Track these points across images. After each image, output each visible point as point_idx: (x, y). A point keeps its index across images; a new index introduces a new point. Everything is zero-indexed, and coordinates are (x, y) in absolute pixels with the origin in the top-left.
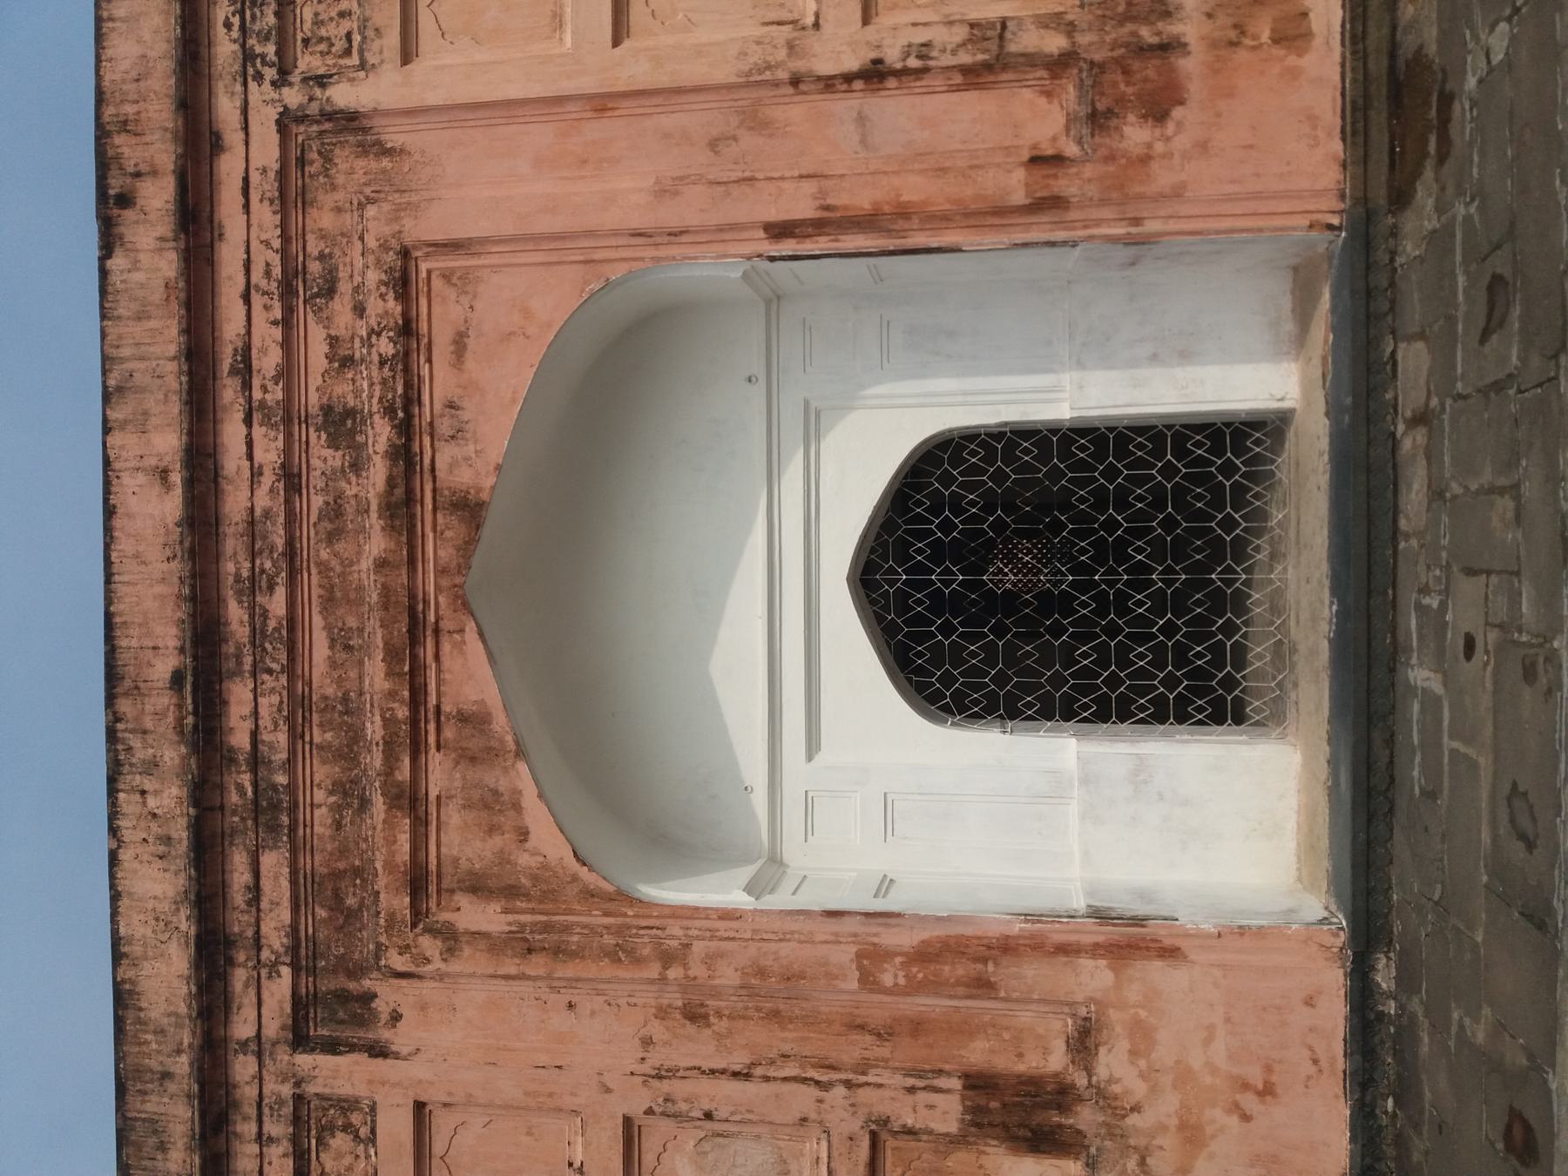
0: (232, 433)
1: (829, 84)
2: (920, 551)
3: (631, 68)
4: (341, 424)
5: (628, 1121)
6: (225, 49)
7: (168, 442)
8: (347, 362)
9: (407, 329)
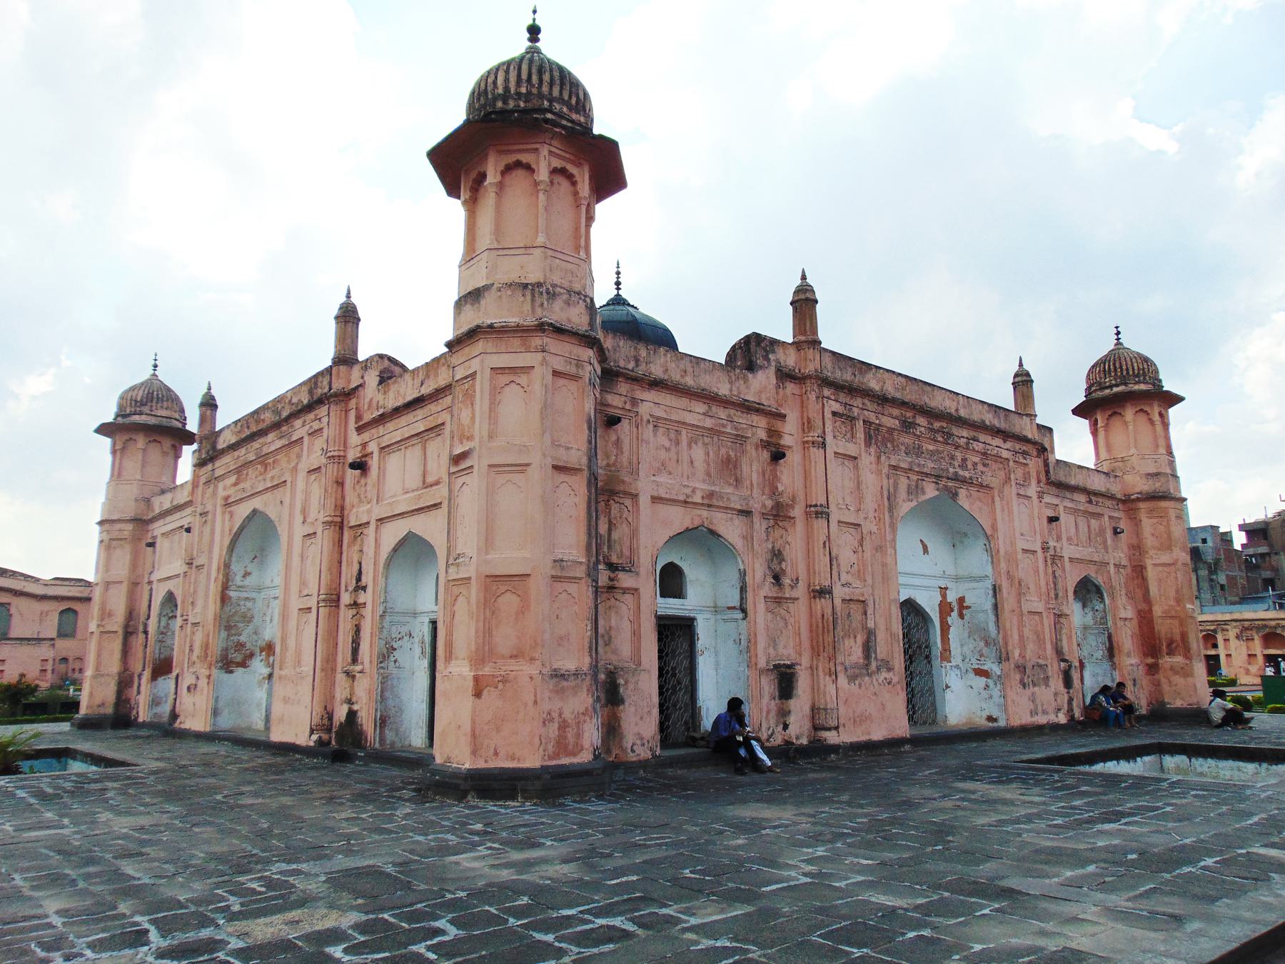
1: (1019, 602)
5: (859, 525)
7: (962, 413)
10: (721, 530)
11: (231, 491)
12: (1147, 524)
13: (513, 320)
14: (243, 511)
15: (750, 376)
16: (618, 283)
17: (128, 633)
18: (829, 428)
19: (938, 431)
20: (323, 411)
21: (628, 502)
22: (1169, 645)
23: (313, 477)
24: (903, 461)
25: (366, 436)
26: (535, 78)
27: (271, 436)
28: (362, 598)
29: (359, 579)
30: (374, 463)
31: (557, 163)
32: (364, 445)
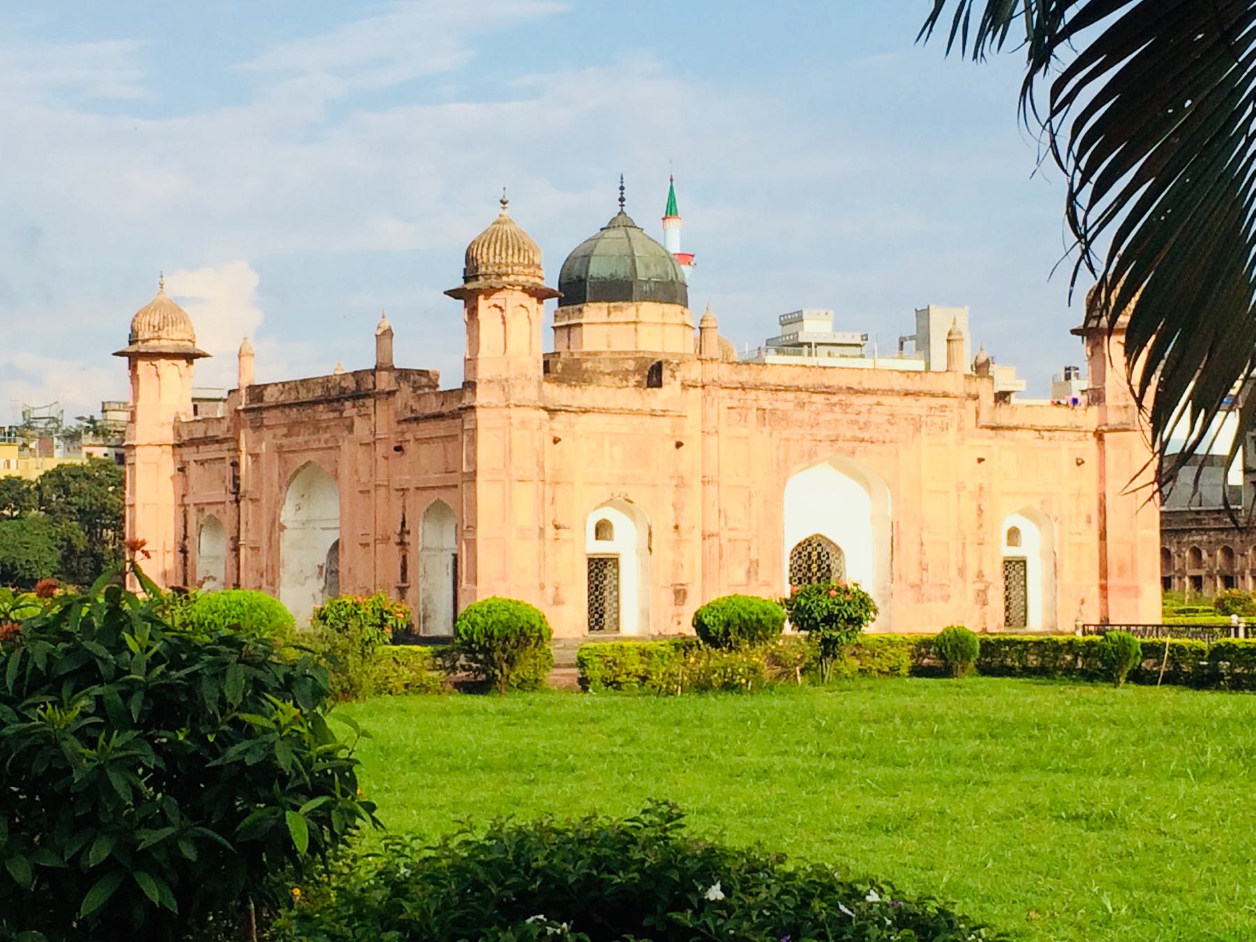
2: (819, 549)
10: (631, 498)
11: (285, 441)
13: (494, 401)
14: (300, 460)
16: (622, 200)
18: (723, 416)
19: (835, 405)
20: (370, 402)
22: (1121, 569)
25: (404, 426)
28: (407, 539)
29: (403, 524)
30: (410, 447)
32: (403, 433)
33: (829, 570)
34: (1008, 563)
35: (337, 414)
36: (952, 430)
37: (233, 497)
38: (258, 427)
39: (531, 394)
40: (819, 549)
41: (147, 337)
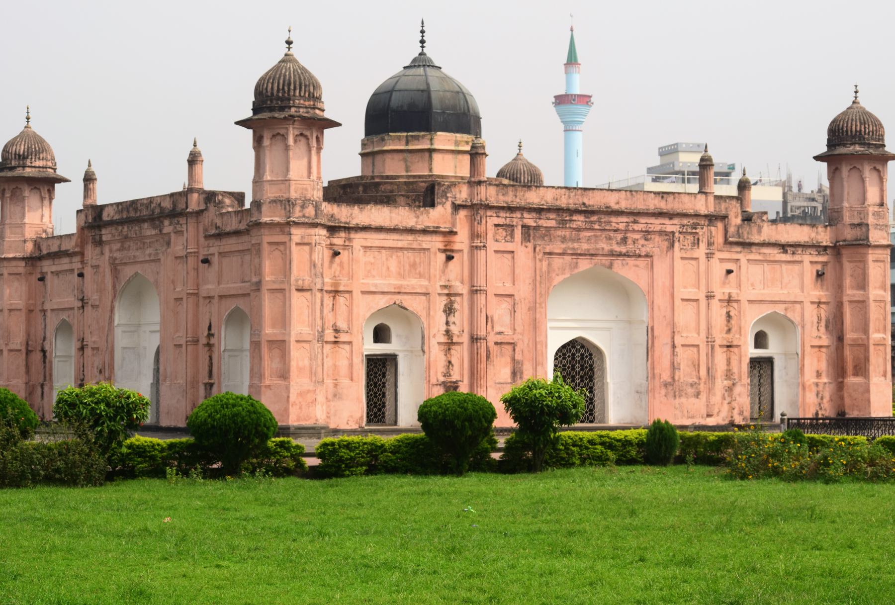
0: (624, 219)
1: (673, 338)
2: (582, 351)
3: (678, 302)
4: (624, 240)
6: (685, 221)
7: (623, 205)
8: (634, 243)
9: (640, 256)
10: (405, 304)
12: (848, 267)
13: (277, 219)
15: (431, 210)
16: (422, 42)
17: (28, 352)
20: (182, 220)
21: (347, 295)
22: (855, 367)
23: (178, 261)
24: (558, 247)
26: (286, 88)
27: (146, 225)
28: (212, 341)
29: (210, 328)
30: (215, 260)
31: (297, 132)
33: (592, 369)
34: (755, 363)
35: (157, 231)
36: (703, 246)
37: (80, 304)
38: (99, 243)
39: (310, 211)
40: (582, 351)
41: (13, 163)
